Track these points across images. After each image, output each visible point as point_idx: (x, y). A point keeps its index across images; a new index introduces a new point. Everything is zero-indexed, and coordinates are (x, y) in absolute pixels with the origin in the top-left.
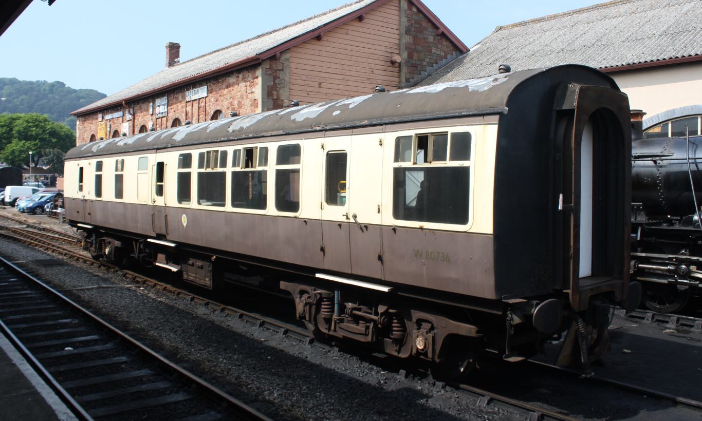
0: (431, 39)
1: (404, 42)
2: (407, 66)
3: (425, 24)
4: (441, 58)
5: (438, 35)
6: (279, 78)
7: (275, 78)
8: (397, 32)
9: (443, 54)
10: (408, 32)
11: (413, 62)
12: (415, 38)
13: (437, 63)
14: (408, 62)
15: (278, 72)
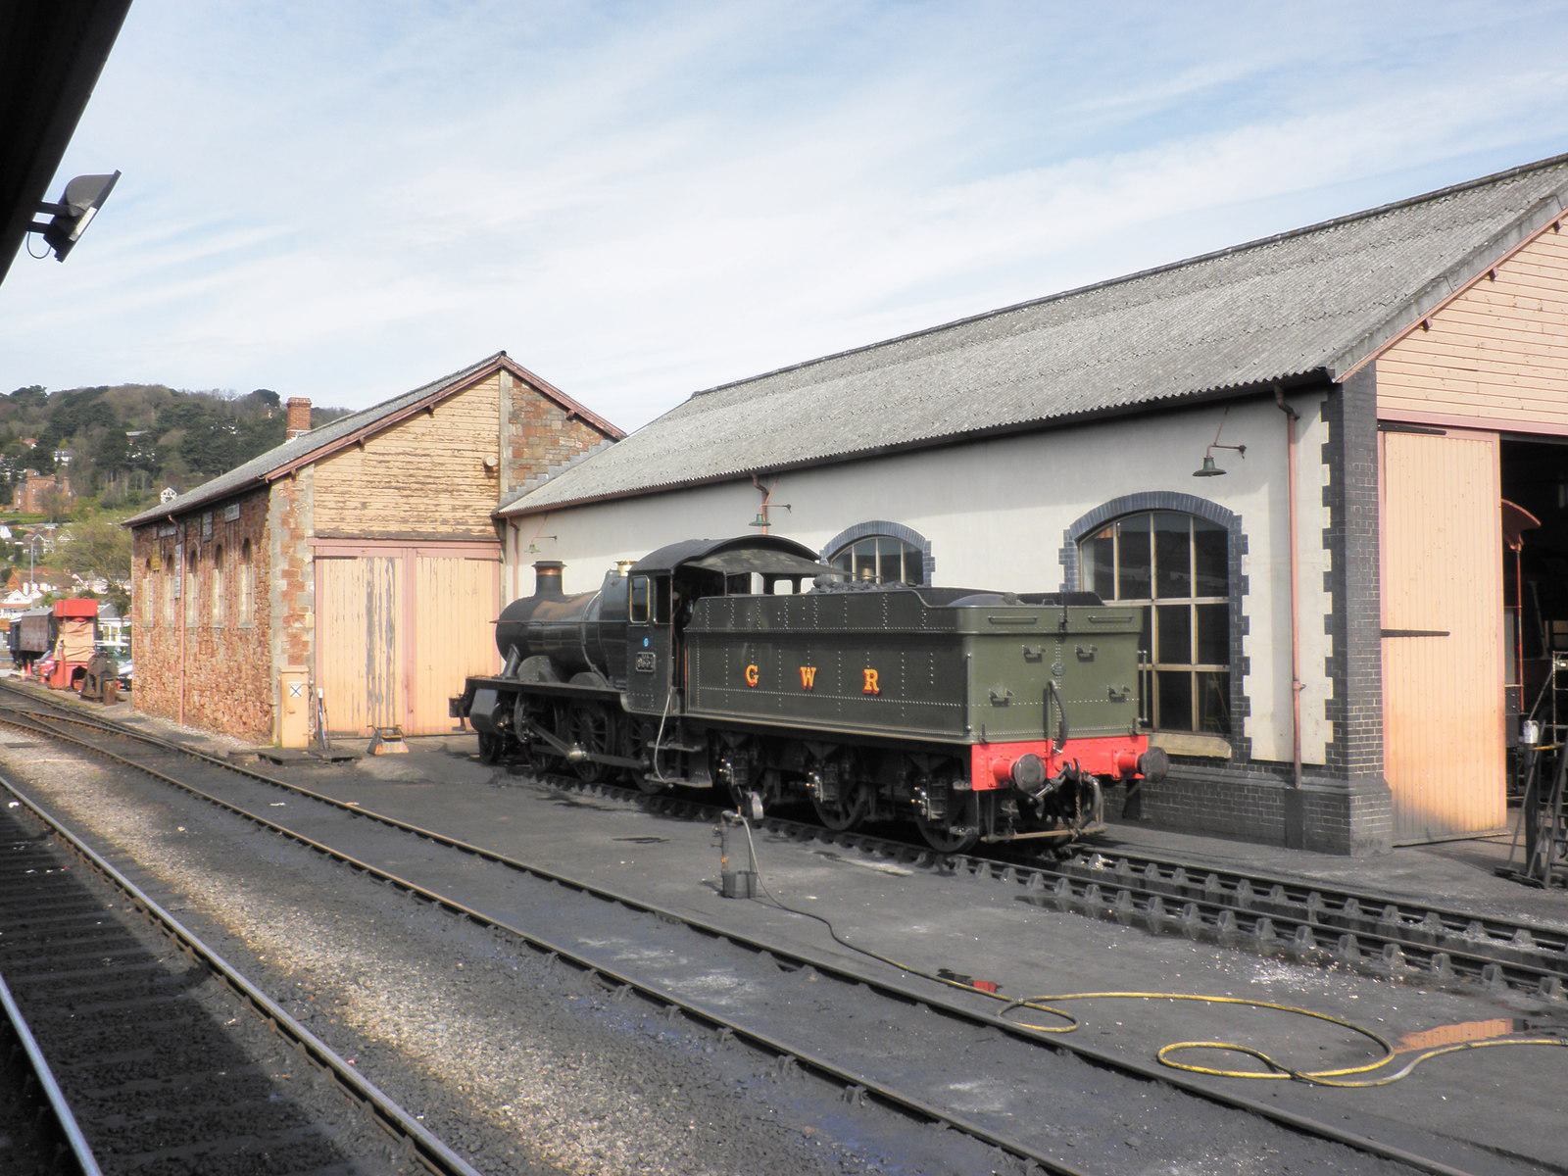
0: (557, 425)
1: (507, 434)
2: (510, 468)
3: (545, 404)
4: (577, 452)
5: (570, 419)
6: (297, 500)
7: (293, 501)
8: (496, 421)
9: (579, 445)
10: (514, 418)
11: (524, 462)
12: (527, 427)
13: (568, 459)
14: (514, 463)
15: (296, 492)
